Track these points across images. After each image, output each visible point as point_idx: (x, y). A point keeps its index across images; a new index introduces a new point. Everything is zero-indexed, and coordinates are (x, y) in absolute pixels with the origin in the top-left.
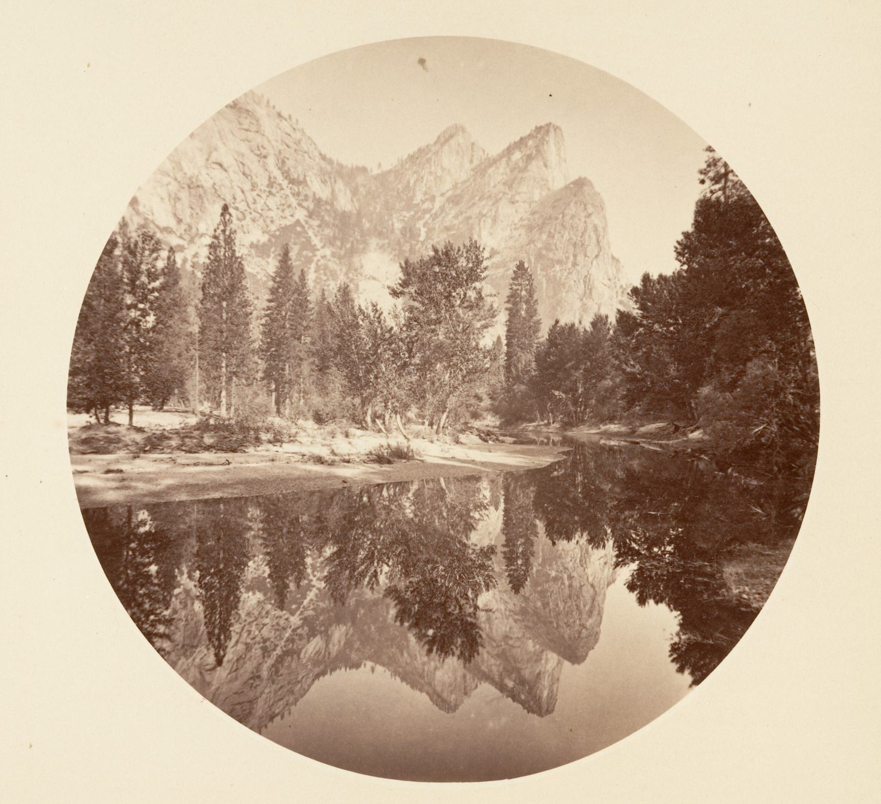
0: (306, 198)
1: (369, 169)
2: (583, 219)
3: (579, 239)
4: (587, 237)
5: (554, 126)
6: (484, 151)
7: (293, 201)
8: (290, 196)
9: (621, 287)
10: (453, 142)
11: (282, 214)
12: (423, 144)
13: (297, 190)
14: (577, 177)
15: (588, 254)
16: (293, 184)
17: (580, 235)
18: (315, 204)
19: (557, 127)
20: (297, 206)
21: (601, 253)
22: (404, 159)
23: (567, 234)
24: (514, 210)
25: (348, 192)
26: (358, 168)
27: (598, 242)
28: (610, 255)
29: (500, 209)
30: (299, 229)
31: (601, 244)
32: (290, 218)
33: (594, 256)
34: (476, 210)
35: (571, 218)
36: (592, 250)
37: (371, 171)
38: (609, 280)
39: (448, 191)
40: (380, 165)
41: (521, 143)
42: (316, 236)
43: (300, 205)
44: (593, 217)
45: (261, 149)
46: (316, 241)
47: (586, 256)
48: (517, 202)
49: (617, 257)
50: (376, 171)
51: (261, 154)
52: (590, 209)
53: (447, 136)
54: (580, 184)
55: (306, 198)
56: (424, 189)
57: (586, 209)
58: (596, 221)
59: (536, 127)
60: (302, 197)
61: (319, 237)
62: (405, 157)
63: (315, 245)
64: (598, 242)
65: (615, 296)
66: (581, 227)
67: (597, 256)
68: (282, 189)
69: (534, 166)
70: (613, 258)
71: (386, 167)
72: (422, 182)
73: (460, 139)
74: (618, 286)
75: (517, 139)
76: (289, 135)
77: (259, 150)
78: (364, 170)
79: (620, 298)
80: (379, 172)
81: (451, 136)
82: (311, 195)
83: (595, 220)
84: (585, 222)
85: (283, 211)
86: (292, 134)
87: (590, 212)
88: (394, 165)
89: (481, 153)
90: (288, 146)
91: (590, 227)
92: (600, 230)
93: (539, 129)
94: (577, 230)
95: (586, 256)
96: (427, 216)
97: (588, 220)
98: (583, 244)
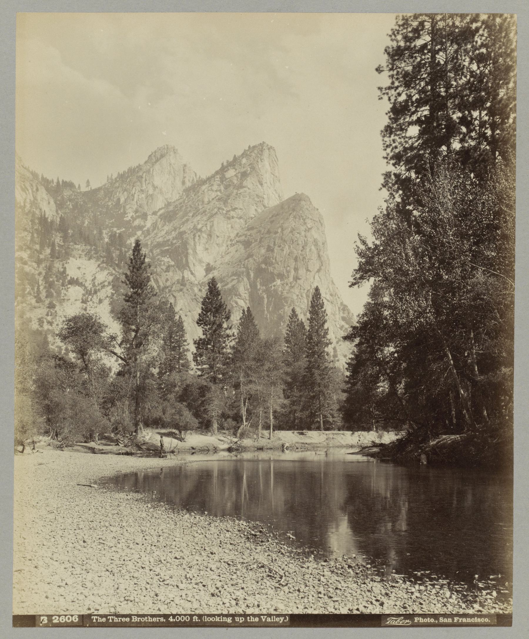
4: (308, 250)
5: (268, 145)
10: (164, 161)
12: (134, 164)
14: (293, 194)
17: (301, 248)
19: (271, 147)
22: (114, 178)
23: (287, 247)
26: (64, 183)
27: (319, 256)
33: (316, 270)
34: (190, 225)
35: (291, 232)
41: (234, 163)
44: (313, 232)
47: (308, 270)
48: (233, 217)
50: (84, 189)
52: (310, 224)
53: (158, 155)
56: (135, 207)
58: (316, 236)
62: (115, 176)
64: (319, 256)
67: (319, 271)
69: (249, 182)
71: (94, 185)
72: (133, 200)
78: (69, 185)
80: (87, 189)
81: (162, 156)
83: (315, 234)
87: (309, 227)
91: (310, 240)
92: (320, 244)
93: (252, 149)
95: (308, 270)
96: (139, 233)
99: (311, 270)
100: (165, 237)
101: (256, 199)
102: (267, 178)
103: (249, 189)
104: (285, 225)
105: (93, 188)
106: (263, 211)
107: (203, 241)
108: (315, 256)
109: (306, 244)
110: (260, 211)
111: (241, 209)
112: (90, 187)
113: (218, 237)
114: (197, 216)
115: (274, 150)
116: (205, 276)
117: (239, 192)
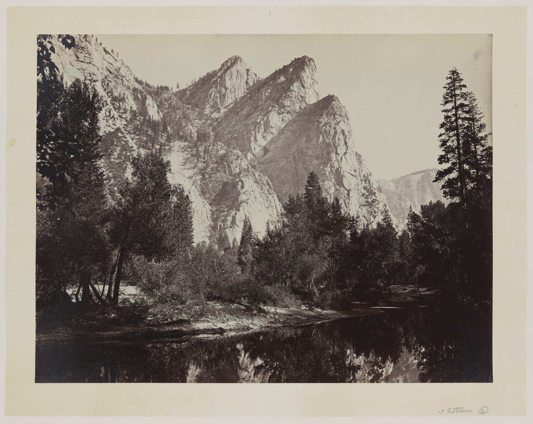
0: (125, 111)
1: (170, 89)
2: (333, 126)
3: (331, 141)
4: (337, 139)
5: (308, 58)
6: (256, 75)
7: (114, 113)
8: (113, 109)
9: (364, 176)
11: (106, 123)
12: (210, 70)
13: (118, 105)
14: (327, 95)
15: (338, 152)
16: (115, 101)
17: (332, 137)
18: (132, 116)
19: (311, 59)
20: (118, 117)
21: (348, 151)
23: (321, 136)
24: (281, 119)
25: (155, 105)
27: (346, 143)
28: (355, 152)
29: (270, 118)
30: (120, 135)
31: (348, 145)
32: (113, 126)
33: (343, 153)
36: (341, 150)
37: (172, 89)
38: (355, 171)
39: (230, 104)
40: (178, 87)
41: (283, 71)
42: (133, 139)
43: (120, 117)
45: (92, 75)
46: (132, 143)
48: (283, 113)
49: (359, 153)
50: (175, 90)
51: (92, 79)
52: (339, 119)
54: (329, 99)
55: (125, 111)
57: (335, 118)
59: (295, 59)
60: (121, 111)
61: (135, 141)
63: (132, 147)
65: (360, 183)
66: (332, 132)
67: (345, 154)
68: (107, 104)
70: (356, 153)
71: (183, 87)
72: (210, 98)
73: (238, 66)
74: (362, 176)
75: (281, 67)
76: (112, 64)
77: (90, 76)
78: (166, 88)
79: (364, 184)
80: (177, 90)
81: (233, 65)
82: (128, 108)
83: (342, 126)
84: (335, 128)
85: (107, 121)
86: (113, 63)
87: (338, 121)
88: (189, 85)
89: (254, 77)
90: (111, 73)
91: (339, 131)
92: (346, 133)
94: (330, 134)
95: (337, 153)
97: (337, 127)
98: (334, 144)
99: (339, 153)
100: (234, 127)
101: (300, 99)
102: (308, 82)
103: (295, 91)
104: (321, 120)
105: (181, 90)
106: (305, 107)
107: (262, 130)
108: (342, 143)
109: (336, 133)
110: (303, 107)
111: (288, 106)
112: (179, 89)
113: (272, 128)
114: (257, 112)
115: (313, 61)
116: (263, 156)
117: (287, 94)
